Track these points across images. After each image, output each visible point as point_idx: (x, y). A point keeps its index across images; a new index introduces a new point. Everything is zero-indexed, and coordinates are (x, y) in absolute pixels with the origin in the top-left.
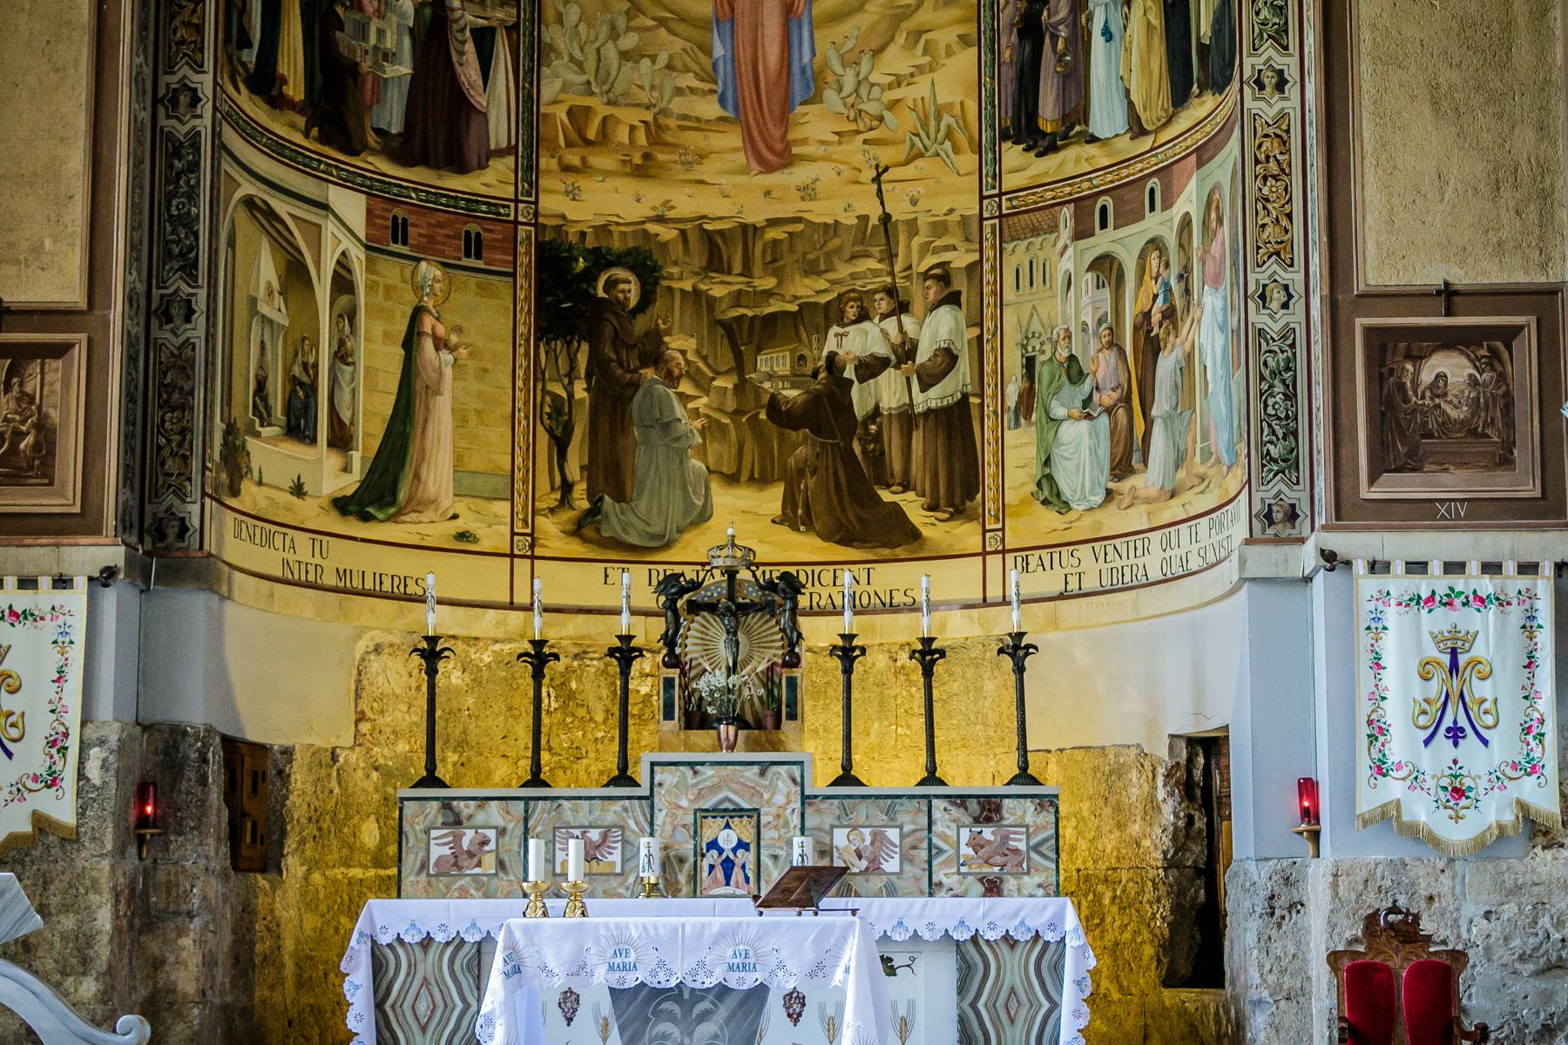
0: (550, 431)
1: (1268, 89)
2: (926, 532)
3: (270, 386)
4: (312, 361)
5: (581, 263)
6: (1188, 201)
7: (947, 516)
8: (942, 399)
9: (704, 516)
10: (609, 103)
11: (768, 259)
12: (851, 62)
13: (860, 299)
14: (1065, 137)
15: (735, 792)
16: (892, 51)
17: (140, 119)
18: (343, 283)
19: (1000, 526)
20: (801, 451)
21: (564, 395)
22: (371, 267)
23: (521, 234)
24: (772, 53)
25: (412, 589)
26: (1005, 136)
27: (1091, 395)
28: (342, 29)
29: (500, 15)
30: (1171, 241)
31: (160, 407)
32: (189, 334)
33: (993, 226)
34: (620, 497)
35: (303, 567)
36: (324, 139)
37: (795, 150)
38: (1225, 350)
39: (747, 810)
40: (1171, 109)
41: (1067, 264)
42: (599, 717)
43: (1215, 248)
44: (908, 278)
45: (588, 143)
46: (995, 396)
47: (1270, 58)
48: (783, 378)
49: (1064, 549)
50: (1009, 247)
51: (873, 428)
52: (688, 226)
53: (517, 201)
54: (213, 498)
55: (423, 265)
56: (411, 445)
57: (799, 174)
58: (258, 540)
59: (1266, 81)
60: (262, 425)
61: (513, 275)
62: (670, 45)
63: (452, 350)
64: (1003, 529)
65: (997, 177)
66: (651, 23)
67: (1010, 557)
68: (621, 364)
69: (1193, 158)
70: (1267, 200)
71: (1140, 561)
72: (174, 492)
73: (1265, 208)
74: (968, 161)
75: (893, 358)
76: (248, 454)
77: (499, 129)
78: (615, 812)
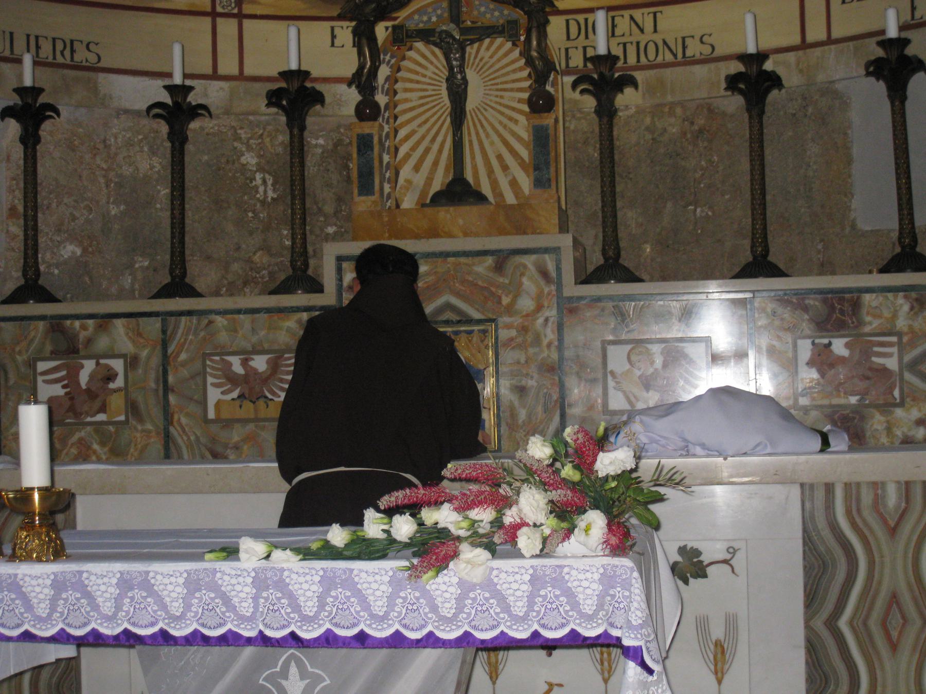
15: (458, 295)
25: (81, 55)
39: (479, 322)
42: (329, 209)
78: (289, 330)
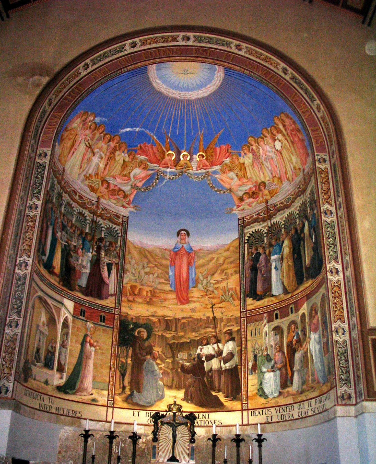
0: (120, 371)
1: (334, 273)
2: (225, 404)
3: (41, 351)
4: (54, 346)
5: (131, 326)
6: (304, 309)
7: (231, 399)
8: (230, 366)
9: (162, 397)
10: (141, 285)
11: (182, 327)
12: (205, 277)
13: (207, 339)
14: (265, 295)
16: (216, 275)
17: (9, 268)
18: (65, 325)
19: (247, 402)
20: (190, 380)
21: (124, 361)
22: (74, 322)
23: (116, 316)
24: (185, 275)
25: (78, 415)
26: (247, 296)
27: (274, 365)
28: (72, 257)
29: (114, 260)
30: (298, 321)
31: (5, 353)
32: (16, 331)
33: (244, 319)
34: (139, 391)
35: (46, 406)
36: (64, 285)
37: (190, 299)
38: (320, 349)
40: (297, 286)
41: (266, 329)
43: (315, 321)
44: (220, 333)
45: (135, 295)
46: (245, 365)
47: (333, 265)
48: (185, 360)
49: (266, 409)
50: (249, 325)
51: (210, 374)
52: (161, 318)
53: (115, 308)
54: (18, 382)
55: (88, 323)
56: (81, 372)
57: (191, 306)
58: (32, 397)
59: (333, 271)
60: (37, 362)
61: (113, 328)
62: (157, 271)
63: (95, 347)
64: (248, 403)
65: (245, 307)
66: (153, 266)
67: (250, 412)
68: (140, 354)
69: (305, 298)
70: (336, 304)
71: (291, 413)
72: (6, 379)
73: (335, 306)
74: (237, 303)
75: (216, 355)
76: (32, 370)
77: (112, 288)
